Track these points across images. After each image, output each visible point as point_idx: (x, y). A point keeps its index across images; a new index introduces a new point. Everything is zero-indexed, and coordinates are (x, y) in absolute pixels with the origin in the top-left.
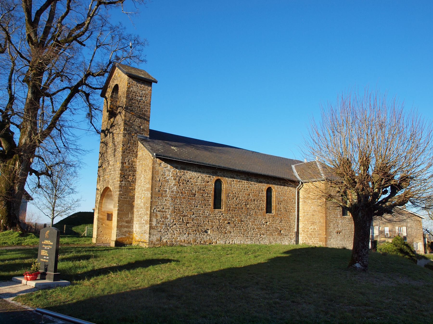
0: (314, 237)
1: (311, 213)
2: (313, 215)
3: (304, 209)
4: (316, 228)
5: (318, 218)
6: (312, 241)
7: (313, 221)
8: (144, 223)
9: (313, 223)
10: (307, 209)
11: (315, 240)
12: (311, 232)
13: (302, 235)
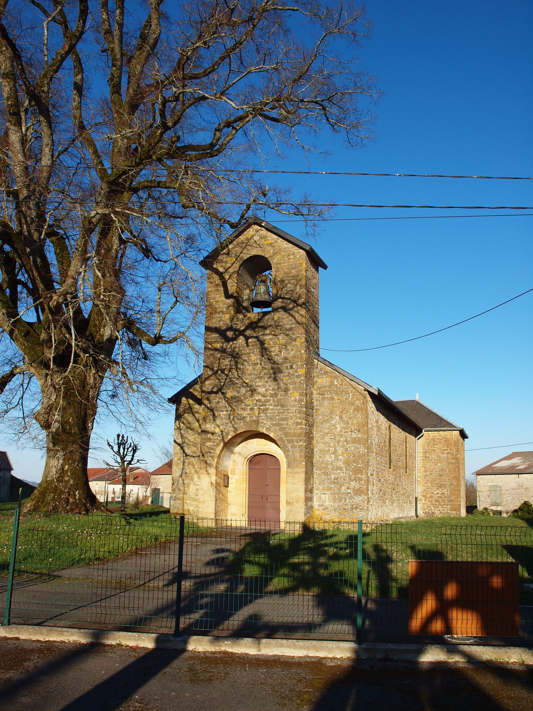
0: (443, 505)
1: (437, 473)
3: (424, 467)
6: (439, 510)
8: (350, 493)
9: (441, 486)
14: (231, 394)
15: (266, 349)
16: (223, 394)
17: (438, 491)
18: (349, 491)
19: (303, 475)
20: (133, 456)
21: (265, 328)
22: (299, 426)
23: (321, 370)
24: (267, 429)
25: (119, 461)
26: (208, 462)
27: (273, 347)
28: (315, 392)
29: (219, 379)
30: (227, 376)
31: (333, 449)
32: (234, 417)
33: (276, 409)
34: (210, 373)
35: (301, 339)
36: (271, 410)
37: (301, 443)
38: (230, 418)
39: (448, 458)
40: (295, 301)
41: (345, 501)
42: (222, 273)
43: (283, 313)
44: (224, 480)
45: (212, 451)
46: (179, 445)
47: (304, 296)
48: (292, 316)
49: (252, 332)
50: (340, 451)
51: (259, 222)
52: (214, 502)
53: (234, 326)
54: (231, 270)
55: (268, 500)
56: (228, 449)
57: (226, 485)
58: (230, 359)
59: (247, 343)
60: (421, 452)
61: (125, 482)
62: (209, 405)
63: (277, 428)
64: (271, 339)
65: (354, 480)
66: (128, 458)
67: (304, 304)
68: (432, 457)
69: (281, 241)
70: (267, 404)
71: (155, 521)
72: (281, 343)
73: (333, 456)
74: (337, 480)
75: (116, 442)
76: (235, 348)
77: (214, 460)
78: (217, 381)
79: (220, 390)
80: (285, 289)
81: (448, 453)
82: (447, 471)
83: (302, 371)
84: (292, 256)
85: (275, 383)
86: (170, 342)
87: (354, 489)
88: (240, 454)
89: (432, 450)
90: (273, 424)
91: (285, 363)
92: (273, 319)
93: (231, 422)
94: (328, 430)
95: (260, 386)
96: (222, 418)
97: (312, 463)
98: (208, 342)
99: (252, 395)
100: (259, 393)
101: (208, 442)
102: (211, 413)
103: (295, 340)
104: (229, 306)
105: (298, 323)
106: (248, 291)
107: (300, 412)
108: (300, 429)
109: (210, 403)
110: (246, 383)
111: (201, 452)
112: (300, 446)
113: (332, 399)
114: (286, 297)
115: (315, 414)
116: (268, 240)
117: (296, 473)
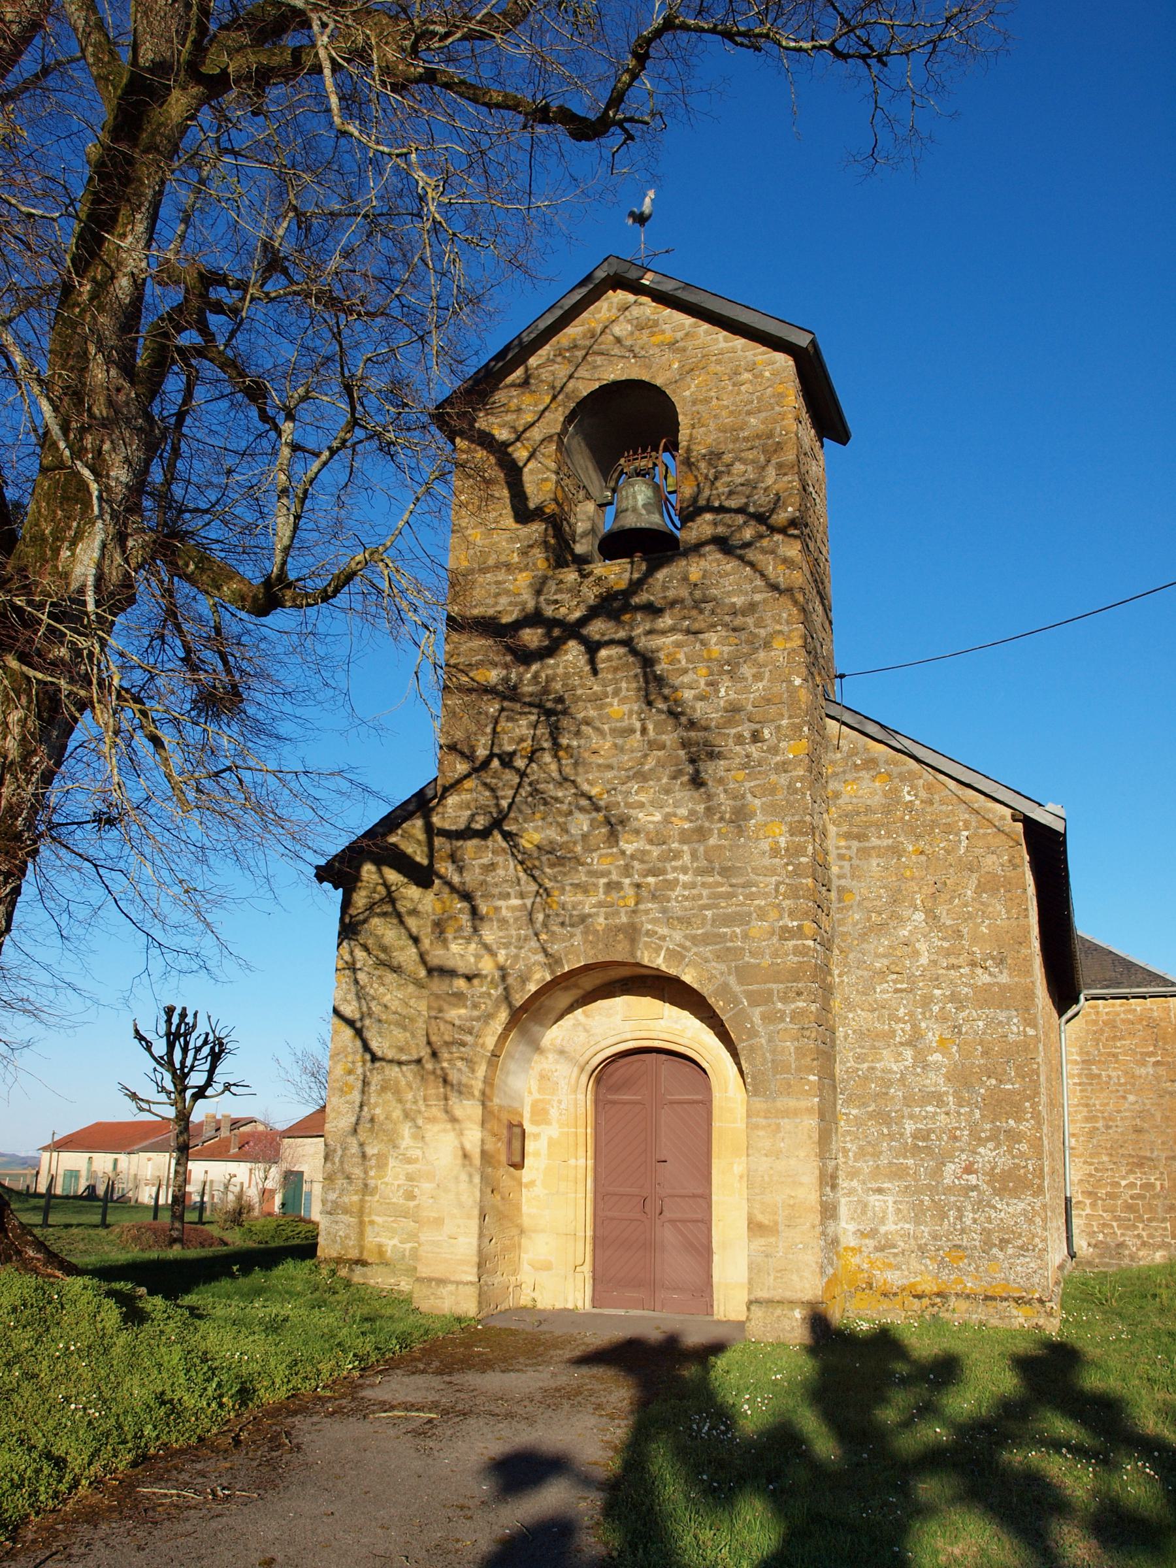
2: (1138, 1131)
3: (1087, 1105)
4: (1158, 1183)
5: (1163, 1143)
6: (1139, 1236)
7: (1142, 1153)
8: (975, 1188)
9: (1140, 1163)
10: (1108, 1104)
11: (1152, 1230)
12: (1132, 1197)
13: (1084, 1213)
14: (537, 837)
15: (660, 680)
16: (507, 836)
17: (1131, 1178)
18: (973, 1179)
19: (811, 1123)
20: (211, 1072)
21: (653, 610)
22: (791, 943)
23: (853, 753)
24: (672, 955)
25: (170, 1087)
26: (453, 1076)
27: (685, 671)
28: (832, 830)
29: (493, 790)
30: (522, 774)
31: (908, 1027)
32: (547, 916)
33: (703, 885)
34: (462, 767)
35: (788, 639)
36: (685, 886)
37: (801, 1004)
38: (531, 921)
39: (1158, 1078)
40: (760, 518)
41: (960, 1218)
42: (506, 445)
43: (719, 556)
44: (510, 1143)
45: (469, 1039)
46: (350, 1023)
47: (796, 500)
48: (752, 565)
49: (611, 624)
50: (932, 1034)
51: (633, 274)
52: (474, 1224)
53: (549, 611)
54: (536, 434)
55: (667, 1214)
56: (524, 1033)
57: (517, 1159)
58: (533, 718)
59: (592, 662)
60: (1076, 1062)
61: (184, 1151)
62: (456, 879)
63: (707, 951)
64: (678, 645)
65: (988, 1139)
66: (197, 1079)
67: (793, 523)
68: (1109, 1076)
69: (707, 333)
70: (668, 866)
71: (258, 1292)
72: (715, 655)
73: (908, 1053)
74: (926, 1138)
75: (162, 1029)
76: (549, 680)
77: (473, 1071)
78: (487, 793)
79: (497, 823)
80: (726, 479)
81: (1157, 1064)
82: (1158, 1116)
83: (793, 750)
84: (747, 376)
85: (696, 795)
86: (325, 597)
87: (991, 1173)
88: (562, 1052)
89: (1109, 1054)
90: (694, 939)
91: (729, 723)
92: (685, 579)
93: (536, 935)
94: (886, 962)
95: (642, 805)
96: (503, 922)
97: (832, 1077)
98: (455, 666)
99: (613, 837)
100: (637, 832)
101: (455, 1006)
102: (465, 904)
103: (767, 645)
104: (531, 546)
105: (774, 587)
106: (590, 507)
107: (794, 892)
108: (797, 951)
109: (460, 870)
110: (590, 798)
111: (429, 1043)
112: (796, 1016)
113: (896, 851)
114: (727, 504)
115: (835, 905)
116: (663, 332)
117: (786, 1113)
